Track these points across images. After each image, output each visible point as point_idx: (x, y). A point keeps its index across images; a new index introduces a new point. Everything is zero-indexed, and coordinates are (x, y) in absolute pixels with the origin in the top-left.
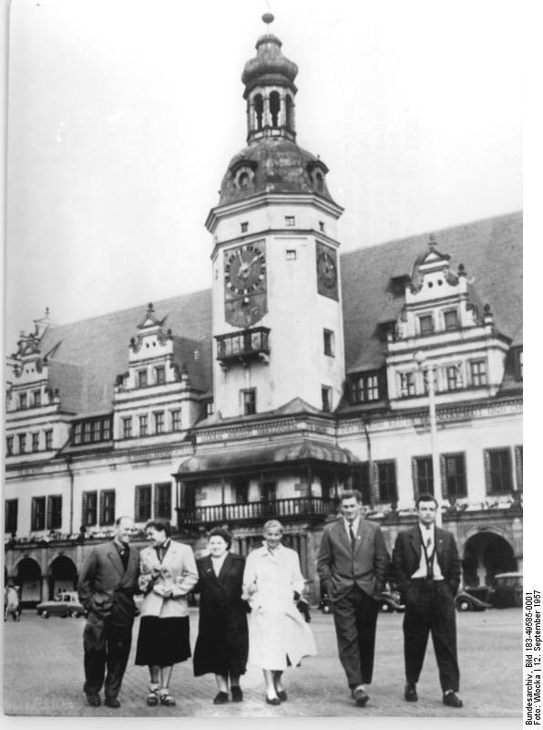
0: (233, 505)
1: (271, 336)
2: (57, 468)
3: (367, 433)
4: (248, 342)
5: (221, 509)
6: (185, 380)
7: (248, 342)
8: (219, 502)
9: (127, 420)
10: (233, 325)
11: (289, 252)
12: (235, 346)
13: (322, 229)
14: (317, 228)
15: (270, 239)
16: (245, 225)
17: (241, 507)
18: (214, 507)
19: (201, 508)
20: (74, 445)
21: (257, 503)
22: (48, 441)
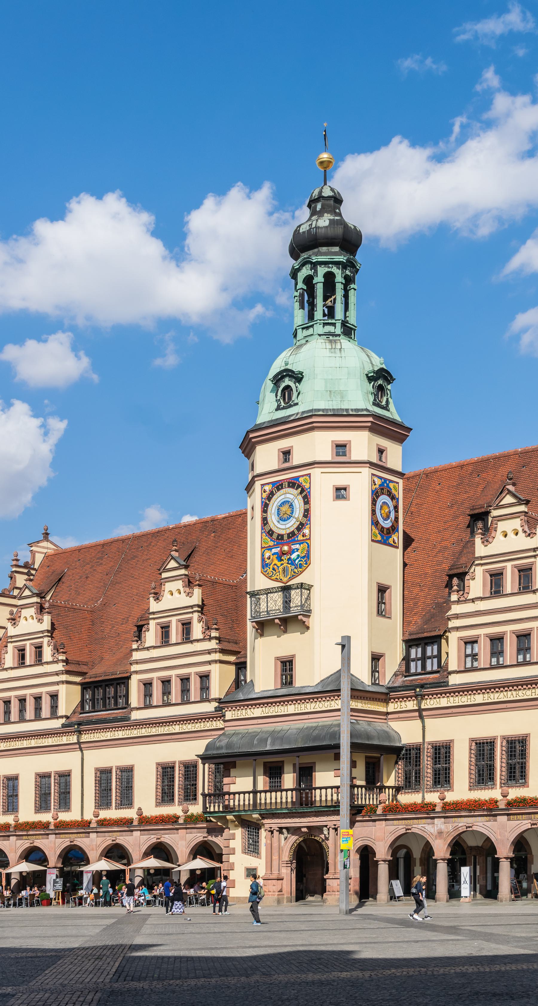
0: (265, 792)
1: (315, 592)
2: (64, 740)
3: (420, 711)
4: (287, 602)
5: (251, 795)
6: (216, 638)
7: (287, 602)
8: (251, 788)
9: (148, 685)
10: (270, 578)
11: (338, 489)
12: (274, 604)
13: (380, 460)
14: (374, 459)
15: (316, 472)
16: (286, 454)
17: (273, 794)
18: (244, 793)
19: (229, 794)
20: (83, 711)
21: (292, 790)
22: (54, 708)
